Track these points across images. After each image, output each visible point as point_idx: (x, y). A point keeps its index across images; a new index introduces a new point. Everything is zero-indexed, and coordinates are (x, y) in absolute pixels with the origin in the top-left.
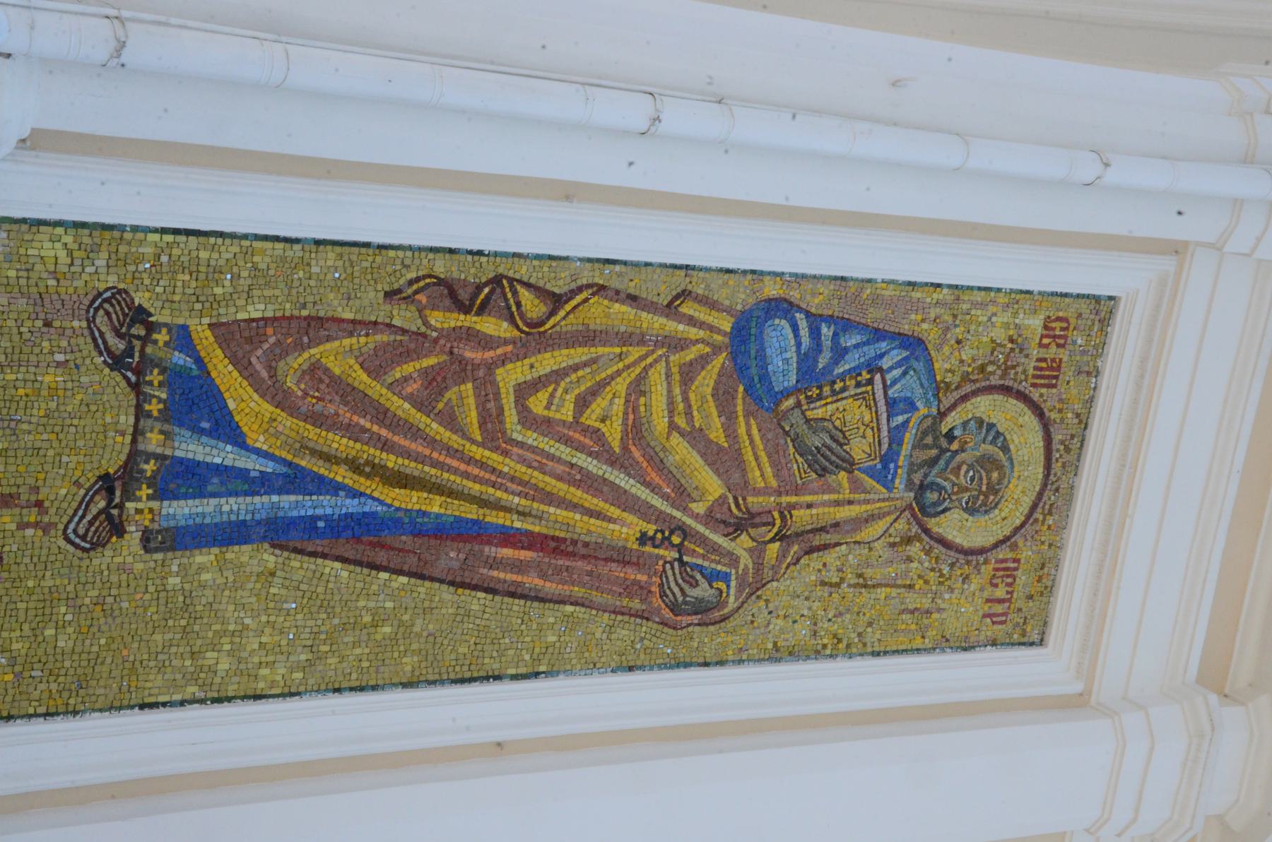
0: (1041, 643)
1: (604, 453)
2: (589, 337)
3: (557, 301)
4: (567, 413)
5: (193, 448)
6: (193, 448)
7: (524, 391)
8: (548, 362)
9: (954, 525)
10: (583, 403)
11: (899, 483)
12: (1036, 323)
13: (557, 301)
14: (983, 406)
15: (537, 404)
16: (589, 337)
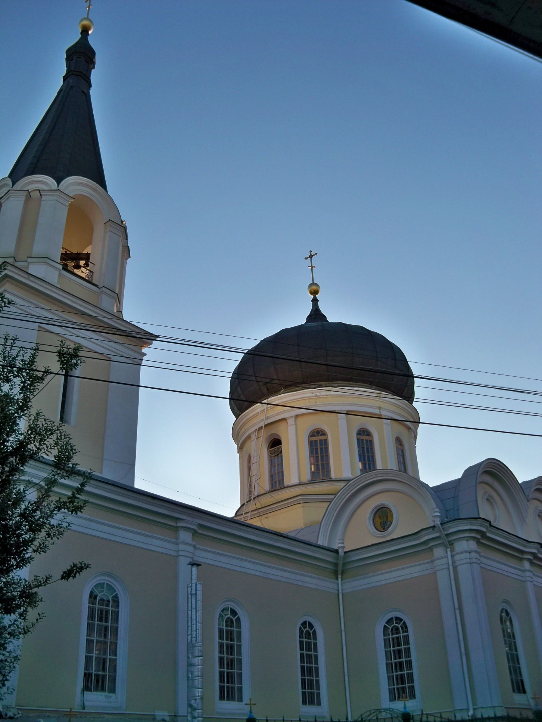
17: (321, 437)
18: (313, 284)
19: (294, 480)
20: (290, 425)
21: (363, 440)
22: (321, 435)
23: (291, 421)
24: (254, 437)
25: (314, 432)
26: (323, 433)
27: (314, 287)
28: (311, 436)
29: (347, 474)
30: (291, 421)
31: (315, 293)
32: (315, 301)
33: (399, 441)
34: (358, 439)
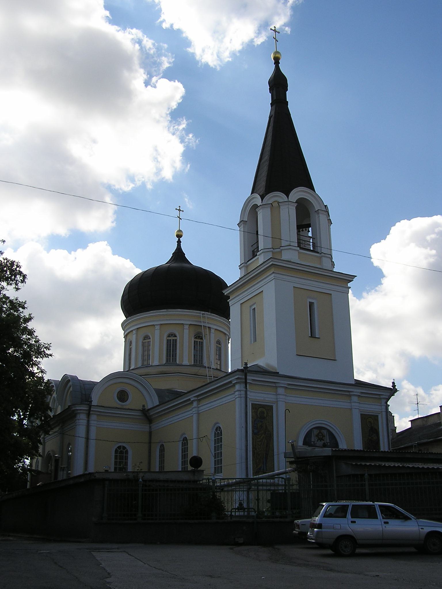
0: (273, 406)
1: (261, 444)
2: (256, 445)
3: (254, 448)
4: (259, 446)
5: (262, 469)
6: (262, 469)
7: (259, 449)
8: (257, 448)
9: (265, 415)
10: (259, 445)
11: (263, 420)
12: (253, 410)
13: (254, 448)
14: (258, 414)
15: (259, 448)
16: (256, 445)
17: (174, 338)
18: (180, 231)
19: (156, 363)
20: (156, 329)
21: (197, 341)
22: (173, 337)
23: (157, 327)
24: (134, 332)
25: (170, 334)
26: (176, 336)
27: (179, 233)
28: (168, 337)
29: (186, 362)
30: (157, 327)
31: (179, 236)
32: (179, 242)
33: (219, 342)
34: (195, 341)
